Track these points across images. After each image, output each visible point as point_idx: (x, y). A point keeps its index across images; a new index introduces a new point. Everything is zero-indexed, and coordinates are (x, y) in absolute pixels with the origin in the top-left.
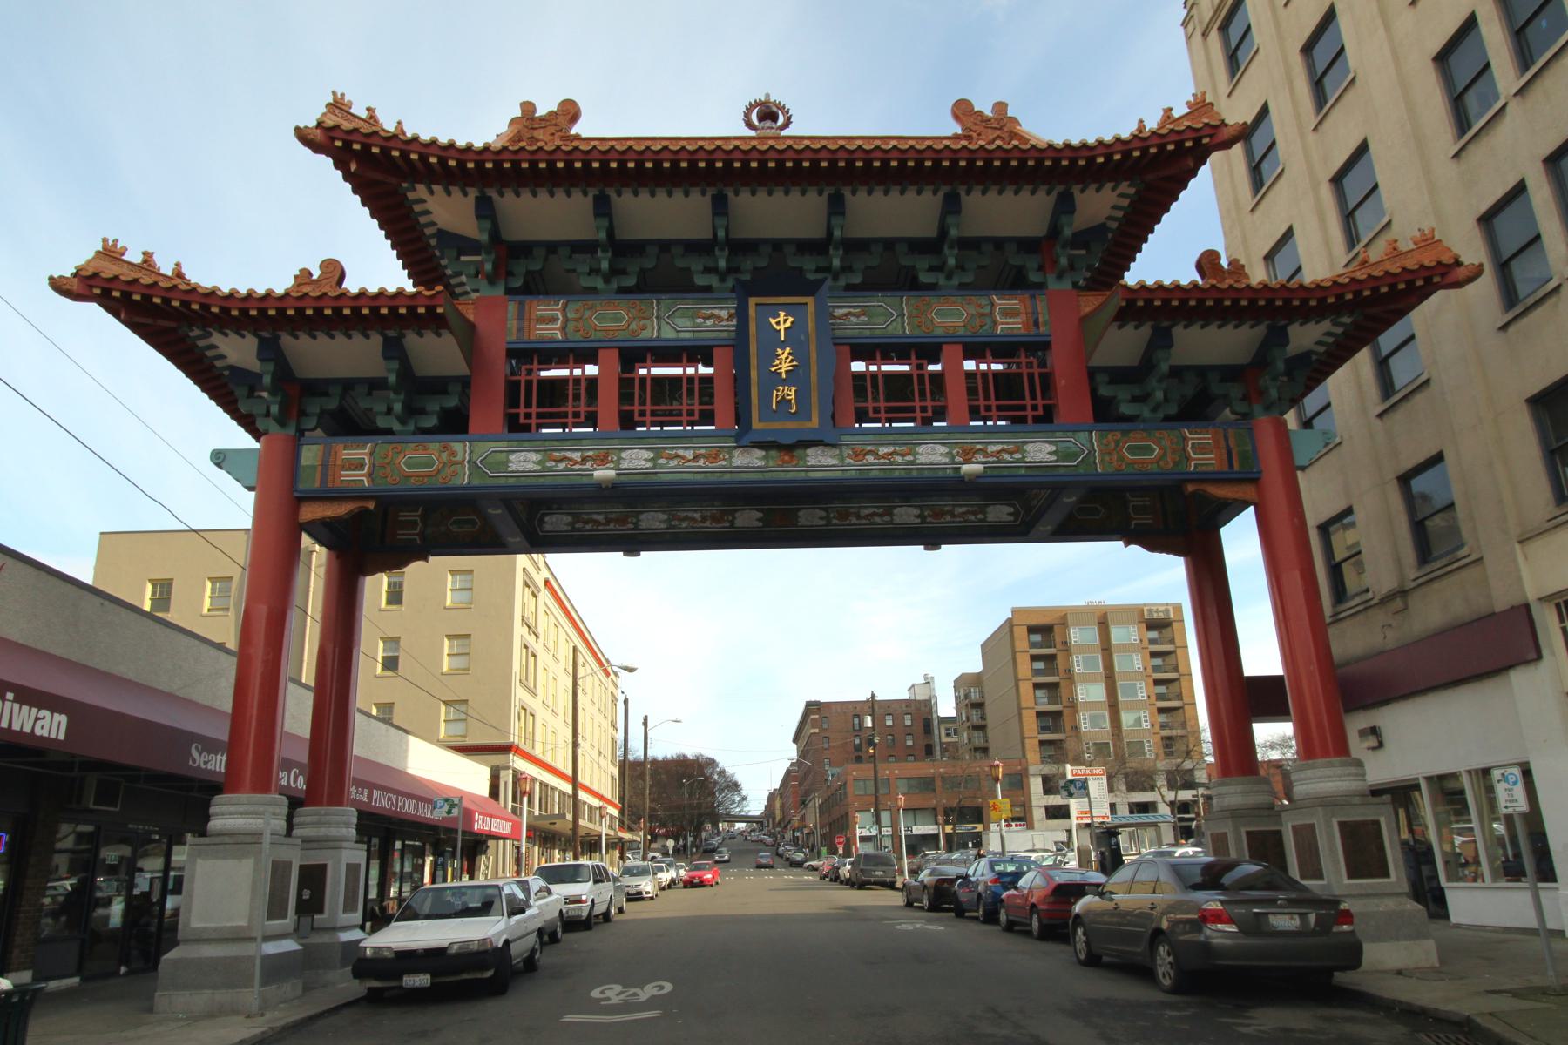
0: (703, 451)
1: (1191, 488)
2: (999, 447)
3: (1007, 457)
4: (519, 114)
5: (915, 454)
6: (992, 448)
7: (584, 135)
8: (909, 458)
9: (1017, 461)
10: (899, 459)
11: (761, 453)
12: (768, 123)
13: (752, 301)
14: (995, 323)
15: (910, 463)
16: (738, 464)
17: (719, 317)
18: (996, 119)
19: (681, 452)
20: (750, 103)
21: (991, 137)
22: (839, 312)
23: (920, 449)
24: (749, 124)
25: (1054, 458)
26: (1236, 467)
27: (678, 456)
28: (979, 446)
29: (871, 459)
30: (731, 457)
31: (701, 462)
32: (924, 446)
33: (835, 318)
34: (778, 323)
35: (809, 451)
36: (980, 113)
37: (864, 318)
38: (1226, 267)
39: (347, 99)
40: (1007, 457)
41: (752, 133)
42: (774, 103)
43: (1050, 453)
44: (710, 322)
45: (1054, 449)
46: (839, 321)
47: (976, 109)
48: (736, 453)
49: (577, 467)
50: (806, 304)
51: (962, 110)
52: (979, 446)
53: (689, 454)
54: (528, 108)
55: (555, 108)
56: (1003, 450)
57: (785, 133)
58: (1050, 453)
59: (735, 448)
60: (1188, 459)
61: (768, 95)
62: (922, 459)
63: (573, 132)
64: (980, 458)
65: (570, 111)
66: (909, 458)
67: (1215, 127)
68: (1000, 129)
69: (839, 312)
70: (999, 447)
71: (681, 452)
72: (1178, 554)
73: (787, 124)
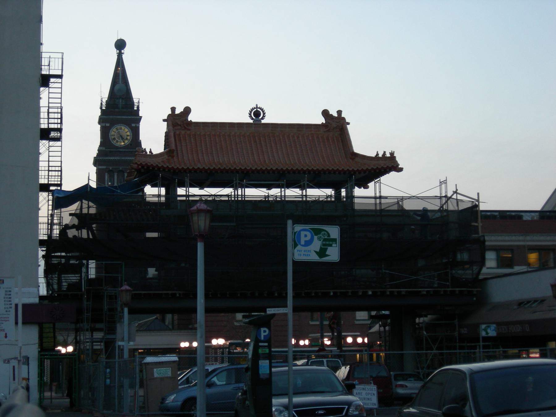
4: (170, 113)
7: (193, 121)
12: (257, 119)
20: (251, 109)
24: (251, 117)
36: (332, 115)
41: (251, 121)
42: (259, 108)
47: (330, 113)
51: (325, 113)
54: (173, 109)
55: (183, 111)
57: (263, 121)
61: (257, 105)
63: (189, 120)
65: (187, 110)
73: (264, 116)
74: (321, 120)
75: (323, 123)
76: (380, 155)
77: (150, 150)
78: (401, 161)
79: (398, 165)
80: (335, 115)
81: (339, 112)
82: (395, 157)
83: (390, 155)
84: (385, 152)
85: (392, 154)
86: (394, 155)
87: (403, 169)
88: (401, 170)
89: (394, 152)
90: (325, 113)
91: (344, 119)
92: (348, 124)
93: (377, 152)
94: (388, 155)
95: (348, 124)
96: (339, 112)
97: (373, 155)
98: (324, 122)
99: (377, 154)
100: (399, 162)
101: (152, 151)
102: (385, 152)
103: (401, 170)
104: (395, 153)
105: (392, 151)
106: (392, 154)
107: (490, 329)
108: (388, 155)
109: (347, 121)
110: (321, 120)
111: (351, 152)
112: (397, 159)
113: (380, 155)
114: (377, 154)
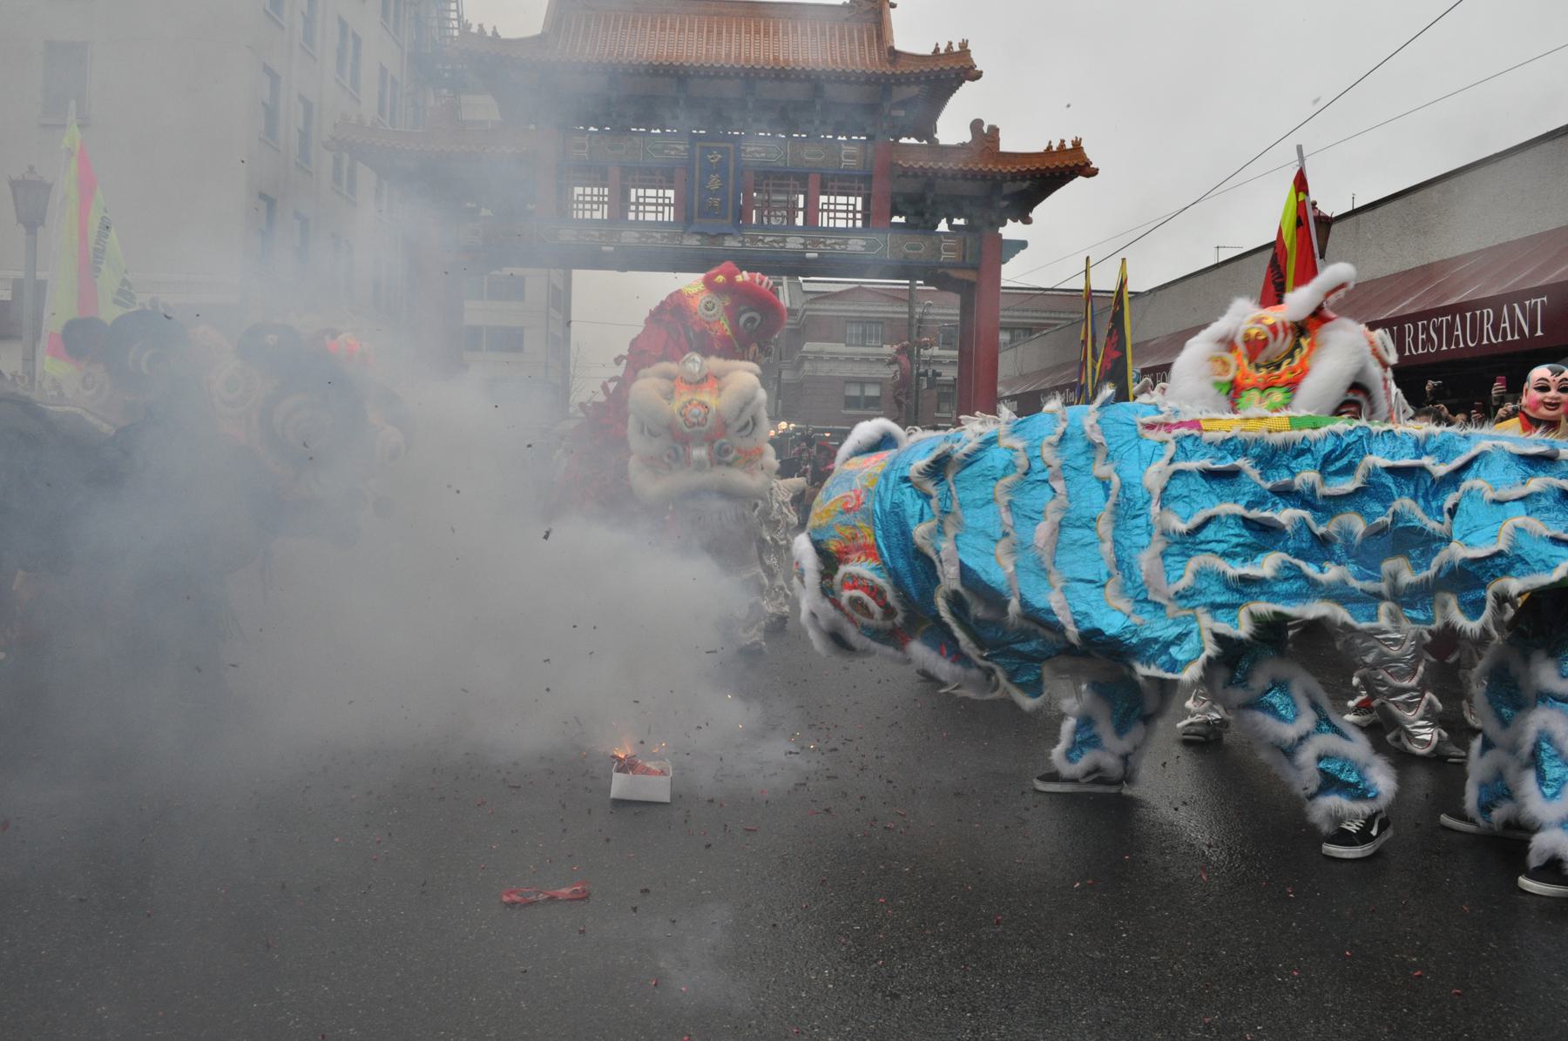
0: (666, 234)
1: (940, 271)
2: (833, 241)
3: (837, 247)
5: (785, 241)
6: (828, 242)
8: (781, 245)
9: (843, 250)
10: (775, 245)
11: (699, 237)
13: (698, 144)
15: (782, 248)
16: (685, 242)
17: (677, 149)
19: (655, 234)
23: (788, 240)
25: (863, 249)
27: (653, 237)
28: (822, 240)
29: (760, 244)
30: (682, 238)
31: (665, 241)
32: (790, 238)
33: (746, 153)
34: (712, 159)
35: (726, 238)
38: (986, 131)
39: (469, 22)
40: (837, 247)
43: (863, 246)
44: (673, 153)
48: (685, 236)
49: (597, 240)
50: (728, 148)
52: (822, 240)
53: (658, 236)
56: (835, 243)
58: (863, 246)
59: (684, 233)
62: (788, 246)
64: (822, 246)
66: (781, 245)
67: (969, 69)
69: (749, 149)
70: (833, 241)
71: (655, 234)
72: (957, 293)
76: (942, 51)
77: (492, 29)
78: (979, 60)
79: (973, 67)
82: (969, 51)
83: (960, 47)
84: (950, 43)
85: (964, 45)
86: (967, 46)
87: (983, 74)
88: (978, 76)
89: (967, 41)
92: (893, 6)
93: (937, 44)
94: (956, 48)
95: (893, 6)
97: (929, 51)
99: (937, 49)
100: (976, 62)
101: (498, 31)
102: (950, 43)
103: (978, 76)
104: (969, 43)
105: (963, 40)
106: (964, 45)
108: (956, 48)
112: (973, 55)
113: (942, 51)
114: (937, 49)
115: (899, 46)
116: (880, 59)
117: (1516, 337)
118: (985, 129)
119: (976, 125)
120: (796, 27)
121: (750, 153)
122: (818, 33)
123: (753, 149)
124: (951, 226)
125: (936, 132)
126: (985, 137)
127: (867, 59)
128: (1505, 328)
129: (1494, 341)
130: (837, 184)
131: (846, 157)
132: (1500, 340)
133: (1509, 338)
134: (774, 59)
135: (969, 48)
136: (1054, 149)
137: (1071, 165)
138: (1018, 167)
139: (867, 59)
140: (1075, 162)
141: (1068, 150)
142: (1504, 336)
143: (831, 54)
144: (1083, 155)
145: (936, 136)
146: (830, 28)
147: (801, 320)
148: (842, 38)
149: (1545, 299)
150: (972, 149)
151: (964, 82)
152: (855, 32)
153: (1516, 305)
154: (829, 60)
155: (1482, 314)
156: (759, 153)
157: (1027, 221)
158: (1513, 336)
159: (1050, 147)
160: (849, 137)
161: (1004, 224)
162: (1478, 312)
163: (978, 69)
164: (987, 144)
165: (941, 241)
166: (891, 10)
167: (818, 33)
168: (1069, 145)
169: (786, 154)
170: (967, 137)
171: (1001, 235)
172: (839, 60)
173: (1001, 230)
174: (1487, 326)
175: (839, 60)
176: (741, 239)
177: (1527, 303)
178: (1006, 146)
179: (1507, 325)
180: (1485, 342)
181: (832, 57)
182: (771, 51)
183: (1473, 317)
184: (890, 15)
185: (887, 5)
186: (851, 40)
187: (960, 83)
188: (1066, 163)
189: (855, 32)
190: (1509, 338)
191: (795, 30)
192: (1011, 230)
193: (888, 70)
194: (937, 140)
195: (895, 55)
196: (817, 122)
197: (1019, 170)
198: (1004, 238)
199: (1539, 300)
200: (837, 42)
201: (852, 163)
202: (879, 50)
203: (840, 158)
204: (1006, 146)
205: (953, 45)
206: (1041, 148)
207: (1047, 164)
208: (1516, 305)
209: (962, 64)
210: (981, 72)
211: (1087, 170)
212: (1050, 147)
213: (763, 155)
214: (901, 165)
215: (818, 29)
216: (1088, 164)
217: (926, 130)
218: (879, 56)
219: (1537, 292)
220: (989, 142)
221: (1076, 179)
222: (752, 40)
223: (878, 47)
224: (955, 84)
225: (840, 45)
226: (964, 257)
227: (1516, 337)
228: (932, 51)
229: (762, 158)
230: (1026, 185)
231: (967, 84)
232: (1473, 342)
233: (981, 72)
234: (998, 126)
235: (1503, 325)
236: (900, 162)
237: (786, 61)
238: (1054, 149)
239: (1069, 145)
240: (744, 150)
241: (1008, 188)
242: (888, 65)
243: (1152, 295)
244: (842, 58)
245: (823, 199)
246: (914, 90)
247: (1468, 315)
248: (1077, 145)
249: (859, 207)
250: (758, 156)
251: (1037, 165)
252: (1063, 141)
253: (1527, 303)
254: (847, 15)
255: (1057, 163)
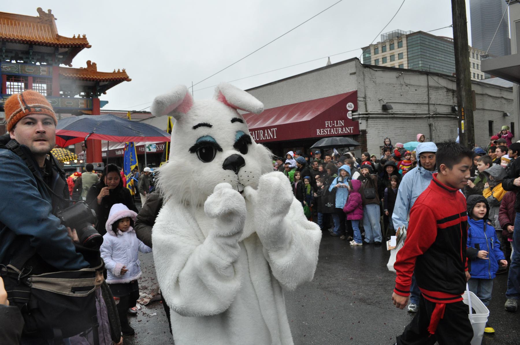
14: (40, 73)
18: (48, 14)
21: (46, 19)
22: (4, 67)
26: (88, 107)
33: (3, 68)
36: (44, 12)
37: (10, 69)
45: (51, 101)
46: (4, 69)
47: (43, 10)
51: (39, 10)
60: (79, 105)
68: (49, 17)
69: (4, 67)
74: (36, 14)
75: (38, 16)
76: (76, 37)
78: (90, 41)
79: (88, 44)
80: (47, 12)
81: (50, 11)
84: (79, 35)
85: (84, 36)
87: (92, 46)
88: (90, 47)
90: (39, 10)
91: (53, 15)
92: (56, 19)
95: (56, 19)
96: (50, 11)
97: (72, 37)
98: (39, 16)
102: (79, 35)
103: (90, 47)
106: (84, 36)
107: (152, 147)
109: (55, 17)
110: (36, 14)
111: (56, 34)
112: (88, 40)
113: (76, 37)
114: (74, 37)
115: (60, 33)
116: (53, 37)
117: (269, 138)
118: (91, 64)
119: (89, 63)
120: (20, 23)
121: (4, 68)
122: (28, 26)
123: (5, 67)
124: (80, 96)
125: (71, 62)
126: (91, 66)
127: (48, 37)
128: (266, 136)
129: (263, 139)
130: (39, 80)
131: (42, 71)
132: (265, 139)
133: (268, 138)
134: (12, 35)
135: (86, 37)
136: (116, 72)
137: (123, 77)
138: (105, 77)
139: (48, 37)
140: (124, 76)
141: (121, 72)
142: (266, 138)
143: (34, 35)
144: (126, 74)
145: (71, 64)
146: (33, 25)
147: (4, 123)
148: (37, 30)
149: (276, 129)
150: (87, 70)
151: (84, 48)
152: (42, 27)
153: (269, 130)
154: (34, 37)
155: (260, 132)
156: (8, 68)
157: (105, 93)
158: (268, 138)
159: (115, 71)
160: (40, 63)
161: (100, 95)
162: (259, 131)
163: (90, 44)
164: (93, 69)
165: (79, 101)
166: (56, 21)
167: (28, 26)
168: (121, 71)
169: (19, 69)
170: (85, 66)
171: (99, 99)
172: (38, 37)
173: (99, 97)
174: (261, 135)
175: (38, 37)
176: (3, 99)
177: (272, 129)
178: (99, 70)
179: (267, 135)
180: (261, 139)
181: (35, 35)
182: (11, 31)
183: (258, 132)
184: (55, 23)
185: (54, 19)
186: (41, 30)
187: (83, 49)
188: (121, 76)
189: (42, 27)
190: (268, 138)
191: (19, 24)
192: (102, 97)
193: (56, 42)
194: (71, 66)
195: (59, 37)
196: (31, 59)
197: (105, 79)
198: (100, 100)
199: (275, 129)
200: (36, 31)
201: (45, 73)
202: (52, 34)
203: (40, 71)
204: (99, 70)
205: (80, 36)
206: (112, 71)
207: (115, 77)
208: (269, 130)
209: (84, 42)
210: (91, 46)
211: (127, 79)
212: (115, 71)
213: (10, 69)
214: (64, 75)
215: (28, 25)
216: (128, 77)
217: (68, 61)
218: (52, 36)
219: (274, 127)
220: (93, 68)
221: (124, 82)
222: (3, 27)
223: (52, 33)
224: (82, 49)
225: (37, 31)
226: (87, 106)
227: (269, 138)
228: (73, 37)
229: (9, 70)
230: (106, 83)
231: (85, 49)
232: (258, 139)
233: (91, 46)
234: (96, 63)
235: (266, 135)
236: (64, 74)
237: (17, 36)
238: (116, 72)
239: (121, 71)
240: (2, 67)
241: (101, 84)
242: (56, 40)
243: (152, 119)
244: (38, 35)
245: (33, 84)
246: (67, 49)
247: (256, 132)
248: (124, 71)
249: (45, 88)
250: (8, 69)
251: (111, 77)
252: (119, 70)
253: (272, 129)
254: (39, 21)
255: (118, 77)
